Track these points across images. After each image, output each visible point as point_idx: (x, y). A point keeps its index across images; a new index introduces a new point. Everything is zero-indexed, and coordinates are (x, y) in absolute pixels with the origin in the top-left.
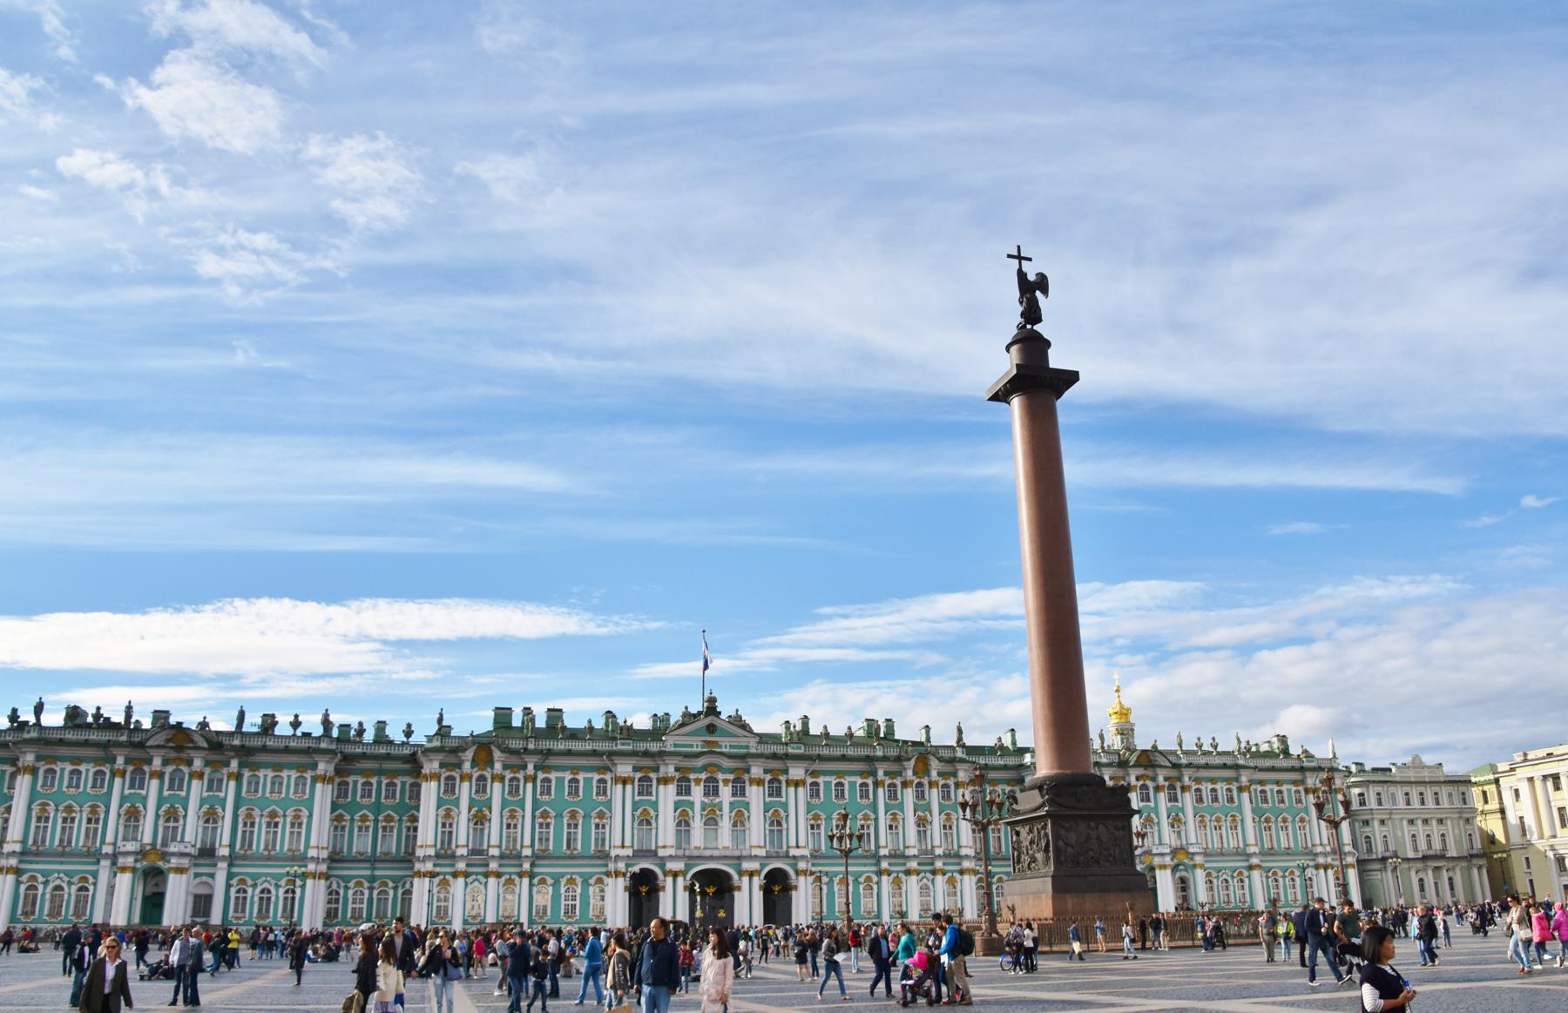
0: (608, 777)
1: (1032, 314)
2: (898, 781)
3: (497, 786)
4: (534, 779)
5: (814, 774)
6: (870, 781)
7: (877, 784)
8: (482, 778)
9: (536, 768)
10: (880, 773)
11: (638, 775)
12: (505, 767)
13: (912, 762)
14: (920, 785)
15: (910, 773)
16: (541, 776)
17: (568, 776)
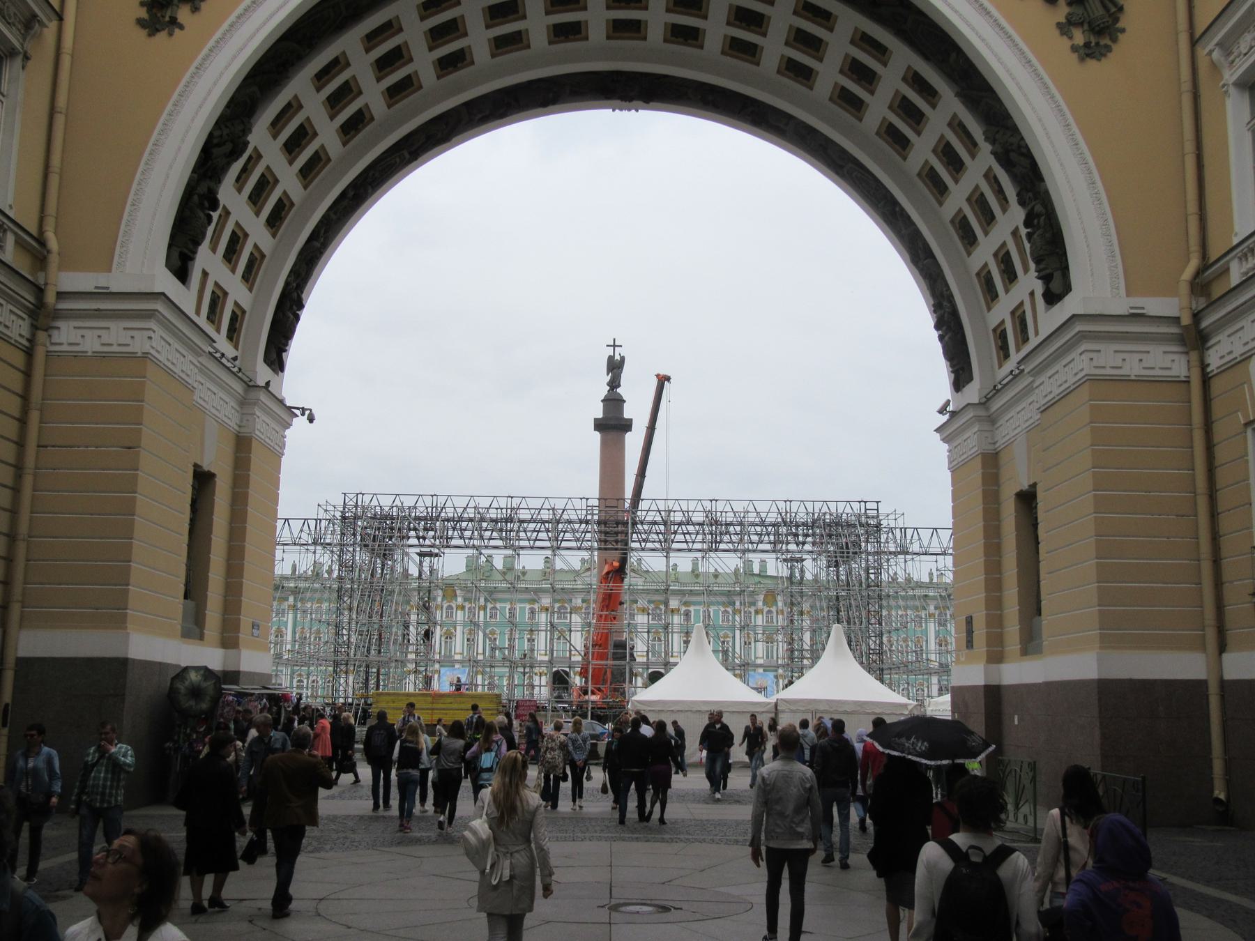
0: (536, 606)
1: (614, 384)
2: (752, 609)
3: (459, 612)
4: (485, 608)
5: (686, 604)
6: (730, 610)
7: (735, 612)
8: (450, 607)
9: (486, 600)
10: (738, 604)
11: (557, 605)
12: (465, 600)
13: (762, 597)
14: (769, 612)
15: (760, 603)
16: (489, 606)
17: (508, 606)
